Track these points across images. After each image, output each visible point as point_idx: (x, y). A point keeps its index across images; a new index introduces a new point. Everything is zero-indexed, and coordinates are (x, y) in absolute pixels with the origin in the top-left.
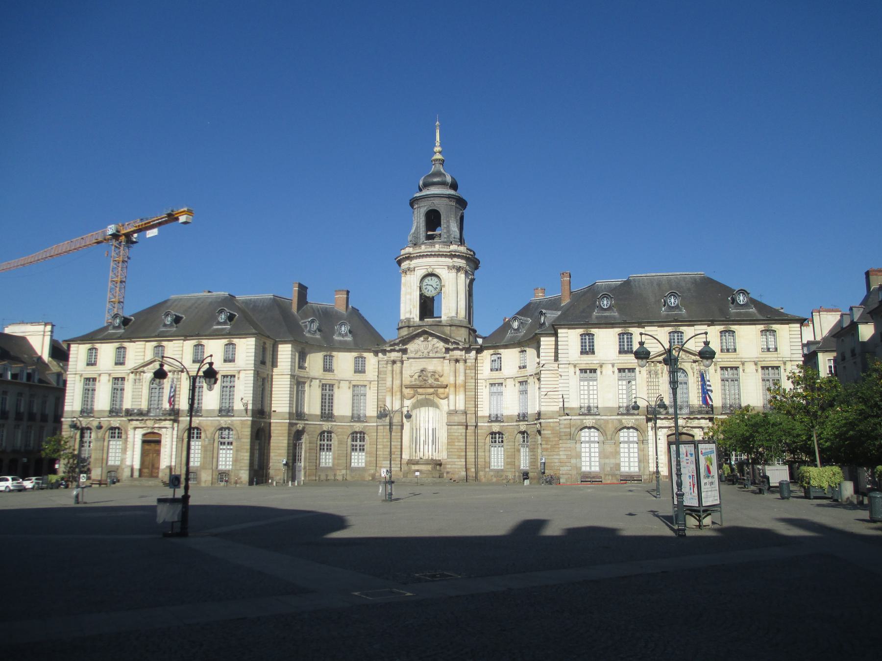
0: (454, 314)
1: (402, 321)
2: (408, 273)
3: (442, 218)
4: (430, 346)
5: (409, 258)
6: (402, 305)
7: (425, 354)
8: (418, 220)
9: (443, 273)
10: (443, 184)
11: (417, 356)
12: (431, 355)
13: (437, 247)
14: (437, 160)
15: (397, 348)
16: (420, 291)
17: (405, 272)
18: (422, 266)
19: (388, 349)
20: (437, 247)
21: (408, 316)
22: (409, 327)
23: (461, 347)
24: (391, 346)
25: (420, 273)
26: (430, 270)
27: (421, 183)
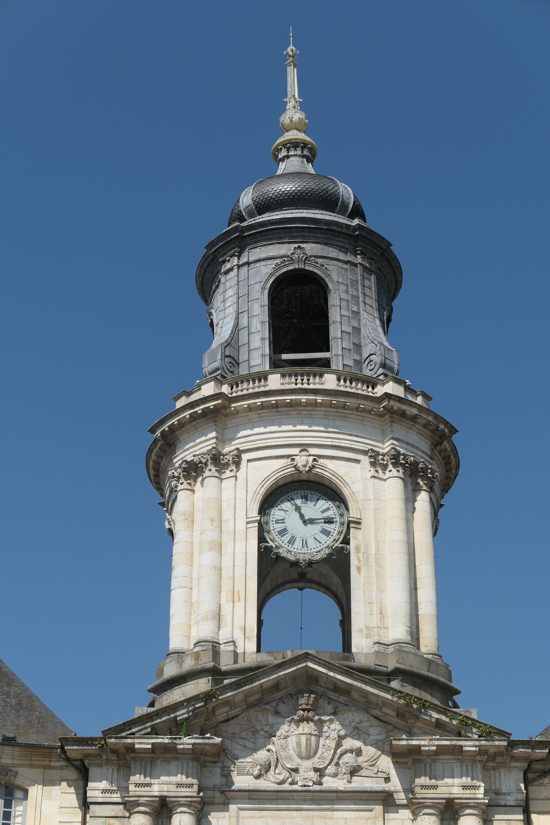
0: (398, 632)
1: (180, 654)
2: (211, 471)
3: (333, 300)
4: (327, 744)
5: (218, 415)
6: (177, 596)
7: (306, 776)
8: (241, 304)
9: (354, 477)
10: (330, 202)
11: (267, 784)
12: (329, 783)
13: (330, 381)
14: (295, 144)
15: (186, 742)
16: (261, 539)
17: (193, 470)
18: (266, 452)
19: (143, 744)
20: (330, 381)
21: (204, 630)
22: (215, 673)
23: (469, 746)
24: (155, 731)
25: (258, 474)
26: (301, 461)
27: (246, 199)
